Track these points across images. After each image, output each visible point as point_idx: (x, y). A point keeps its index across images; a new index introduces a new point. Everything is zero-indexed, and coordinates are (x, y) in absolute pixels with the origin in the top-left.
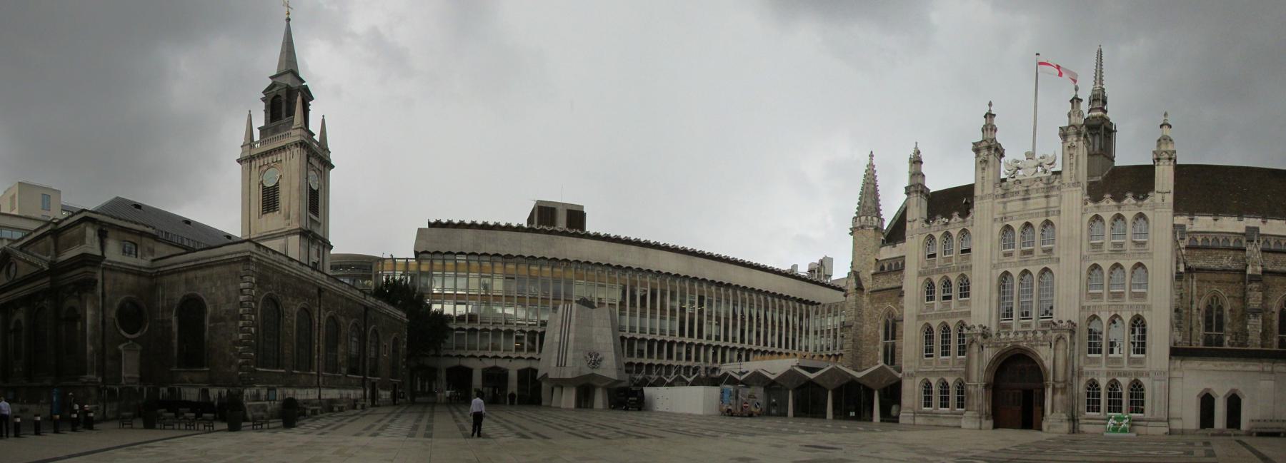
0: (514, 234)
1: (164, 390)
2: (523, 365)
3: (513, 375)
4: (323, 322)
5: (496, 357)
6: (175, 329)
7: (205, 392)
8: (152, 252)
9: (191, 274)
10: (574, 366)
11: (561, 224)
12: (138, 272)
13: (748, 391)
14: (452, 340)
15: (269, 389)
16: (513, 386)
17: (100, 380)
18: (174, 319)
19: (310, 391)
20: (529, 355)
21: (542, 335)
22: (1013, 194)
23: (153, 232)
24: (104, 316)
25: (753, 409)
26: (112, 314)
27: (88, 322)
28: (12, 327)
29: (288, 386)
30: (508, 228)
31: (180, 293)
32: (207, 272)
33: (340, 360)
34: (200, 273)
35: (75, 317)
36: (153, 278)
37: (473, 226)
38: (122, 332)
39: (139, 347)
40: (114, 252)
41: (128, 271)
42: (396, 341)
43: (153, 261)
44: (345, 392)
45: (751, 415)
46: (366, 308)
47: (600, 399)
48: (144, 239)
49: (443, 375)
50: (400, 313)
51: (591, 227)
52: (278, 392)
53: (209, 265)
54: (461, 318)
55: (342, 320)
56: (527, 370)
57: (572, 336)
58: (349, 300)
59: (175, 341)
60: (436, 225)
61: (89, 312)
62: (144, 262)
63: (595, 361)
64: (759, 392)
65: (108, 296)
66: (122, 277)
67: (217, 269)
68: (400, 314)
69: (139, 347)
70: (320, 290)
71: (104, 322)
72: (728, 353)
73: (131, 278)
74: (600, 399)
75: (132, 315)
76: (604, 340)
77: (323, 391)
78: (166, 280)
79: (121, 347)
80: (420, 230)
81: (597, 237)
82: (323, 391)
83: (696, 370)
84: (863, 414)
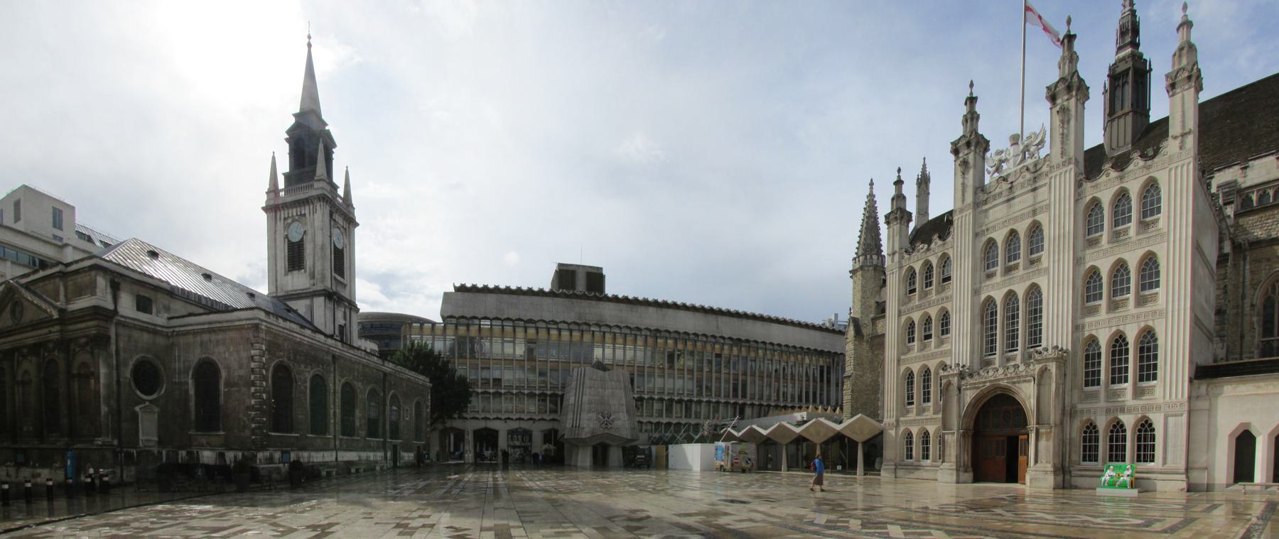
0: (535, 299)
2: (547, 426)
3: (537, 437)
5: (520, 419)
6: (192, 392)
9: (206, 337)
10: (588, 424)
11: (581, 286)
13: (739, 447)
14: (476, 403)
16: (538, 446)
18: (190, 381)
20: (552, 416)
21: (562, 396)
22: (995, 198)
25: (744, 465)
27: (102, 380)
28: (19, 378)
30: (530, 292)
31: (196, 356)
32: (220, 336)
34: (214, 337)
37: (497, 290)
39: (156, 410)
42: (418, 405)
44: (364, 455)
45: (744, 471)
47: (615, 455)
49: (470, 438)
50: (422, 377)
51: (610, 290)
53: (221, 330)
54: (486, 382)
56: (550, 431)
57: (586, 399)
60: (462, 289)
61: (103, 371)
63: (606, 419)
64: (751, 448)
67: (233, 334)
68: (423, 380)
69: (156, 410)
72: (721, 407)
74: (615, 455)
76: (618, 399)
80: (446, 295)
81: (615, 299)
83: (697, 425)
84: (850, 467)
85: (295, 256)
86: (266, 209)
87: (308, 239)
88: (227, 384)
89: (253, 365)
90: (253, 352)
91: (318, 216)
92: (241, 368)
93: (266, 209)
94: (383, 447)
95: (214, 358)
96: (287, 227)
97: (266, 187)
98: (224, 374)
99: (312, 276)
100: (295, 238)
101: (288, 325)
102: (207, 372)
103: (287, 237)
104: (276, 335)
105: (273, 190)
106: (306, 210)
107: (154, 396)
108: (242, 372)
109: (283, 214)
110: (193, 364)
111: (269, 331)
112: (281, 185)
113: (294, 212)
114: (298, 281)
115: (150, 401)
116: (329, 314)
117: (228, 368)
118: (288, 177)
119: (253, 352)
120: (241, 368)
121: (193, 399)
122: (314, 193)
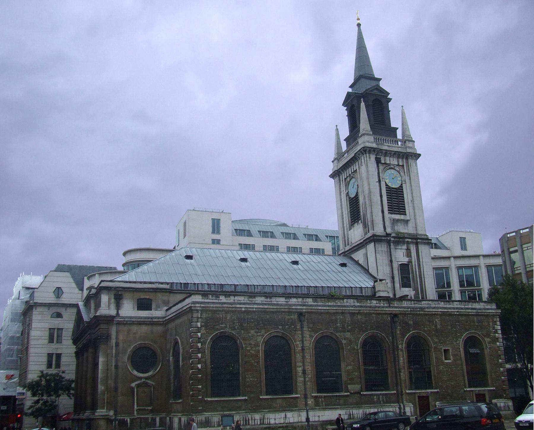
1: (168, 418)
4: (309, 343)
7: (180, 420)
8: (166, 303)
12: (151, 322)
15: (223, 416)
17: (112, 413)
19: (289, 414)
23: (168, 287)
24: (117, 361)
26: (126, 359)
29: (256, 410)
33: (344, 377)
35: (96, 365)
36: (165, 323)
38: (135, 373)
40: (129, 310)
41: (141, 322)
43: (167, 310)
46: (395, 316)
48: (159, 295)
52: (236, 418)
55: (344, 337)
58: (352, 314)
59: (172, 377)
62: (157, 313)
65: (121, 345)
66: (135, 328)
70: (301, 314)
71: (117, 367)
73: (145, 329)
75: (143, 358)
77: (311, 414)
79: (133, 385)
82: (311, 414)
85: (355, 211)
86: (332, 176)
87: (360, 191)
88: (183, 361)
91: (367, 167)
93: (332, 176)
94: (398, 399)
96: (347, 185)
97: (332, 155)
98: (181, 351)
99: (365, 226)
100: (352, 195)
101: (232, 299)
103: (348, 194)
104: (214, 312)
105: (340, 155)
106: (355, 167)
107: (150, 373)
109: (343, 176)
111: (204, 310)
112: (344, 147)
113: (349, 171)
114: (357, 234)
115: (146, 378)
116: (383, 260)
118: (348, 140)
120: (187, 344)
122: (359, 148)
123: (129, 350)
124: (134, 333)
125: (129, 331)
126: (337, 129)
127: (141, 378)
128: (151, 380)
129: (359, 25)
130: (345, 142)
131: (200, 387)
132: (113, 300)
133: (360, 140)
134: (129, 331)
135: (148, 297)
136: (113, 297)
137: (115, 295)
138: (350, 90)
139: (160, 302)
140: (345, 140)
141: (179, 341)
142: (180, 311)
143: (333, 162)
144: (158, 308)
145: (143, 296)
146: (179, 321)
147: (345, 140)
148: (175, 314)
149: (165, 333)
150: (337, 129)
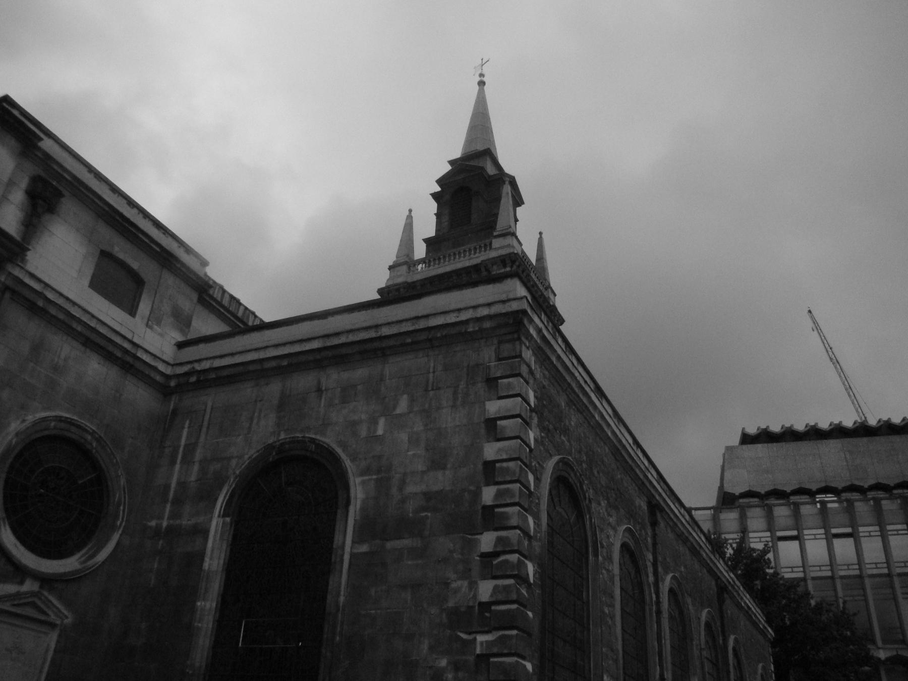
6: (214, 559)
8: (183, 321)
12: (125, 360)
18: (216, 524)
39: (62, 613)
43: (180, 345)
48: (169, 279)
59: (207, 606)
66: (64, 348)
69: (62, 613)
73: (94, 368)
78: (211, 400)
89: (491, 451)
90: (493, 407)
92: (437, 463)
95: (329, 440)
98: (359, 491)
102: (291, 493)
108: (441, 481)
110: (236, 468)
115: (47, 581)
117: (382, 474)
118: (429, 242)
119: (493, 407)
121: (216, 586)
123: (15, 426)
124: (55, 368)
125: (37, 348)
126: (410, 217)
127: (20, 572)
128: (60, 598)
129: (482, 83)
130: (424, 245)
131: (529, 666)
132: (18, 196)
133: (496, 243)
134: (37, 348)
135: (135, 265)
136: (24, 183)
137: (35, 180)
138: (449, 168)
139: (166, 308)
140: (425, 240)
141: (343, 456)
142: (386, 331)
143: (390, 268)
144: (153, 320)
145: (123, 251)
146: (333, 378)
147: (425, 240)
148: (315, 345)
149: (166, 424)
150: (410, 217)
